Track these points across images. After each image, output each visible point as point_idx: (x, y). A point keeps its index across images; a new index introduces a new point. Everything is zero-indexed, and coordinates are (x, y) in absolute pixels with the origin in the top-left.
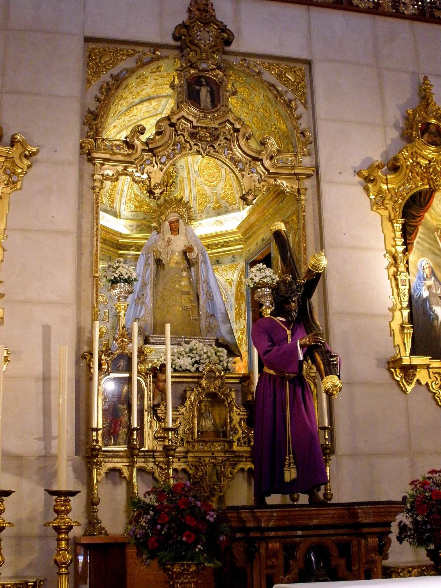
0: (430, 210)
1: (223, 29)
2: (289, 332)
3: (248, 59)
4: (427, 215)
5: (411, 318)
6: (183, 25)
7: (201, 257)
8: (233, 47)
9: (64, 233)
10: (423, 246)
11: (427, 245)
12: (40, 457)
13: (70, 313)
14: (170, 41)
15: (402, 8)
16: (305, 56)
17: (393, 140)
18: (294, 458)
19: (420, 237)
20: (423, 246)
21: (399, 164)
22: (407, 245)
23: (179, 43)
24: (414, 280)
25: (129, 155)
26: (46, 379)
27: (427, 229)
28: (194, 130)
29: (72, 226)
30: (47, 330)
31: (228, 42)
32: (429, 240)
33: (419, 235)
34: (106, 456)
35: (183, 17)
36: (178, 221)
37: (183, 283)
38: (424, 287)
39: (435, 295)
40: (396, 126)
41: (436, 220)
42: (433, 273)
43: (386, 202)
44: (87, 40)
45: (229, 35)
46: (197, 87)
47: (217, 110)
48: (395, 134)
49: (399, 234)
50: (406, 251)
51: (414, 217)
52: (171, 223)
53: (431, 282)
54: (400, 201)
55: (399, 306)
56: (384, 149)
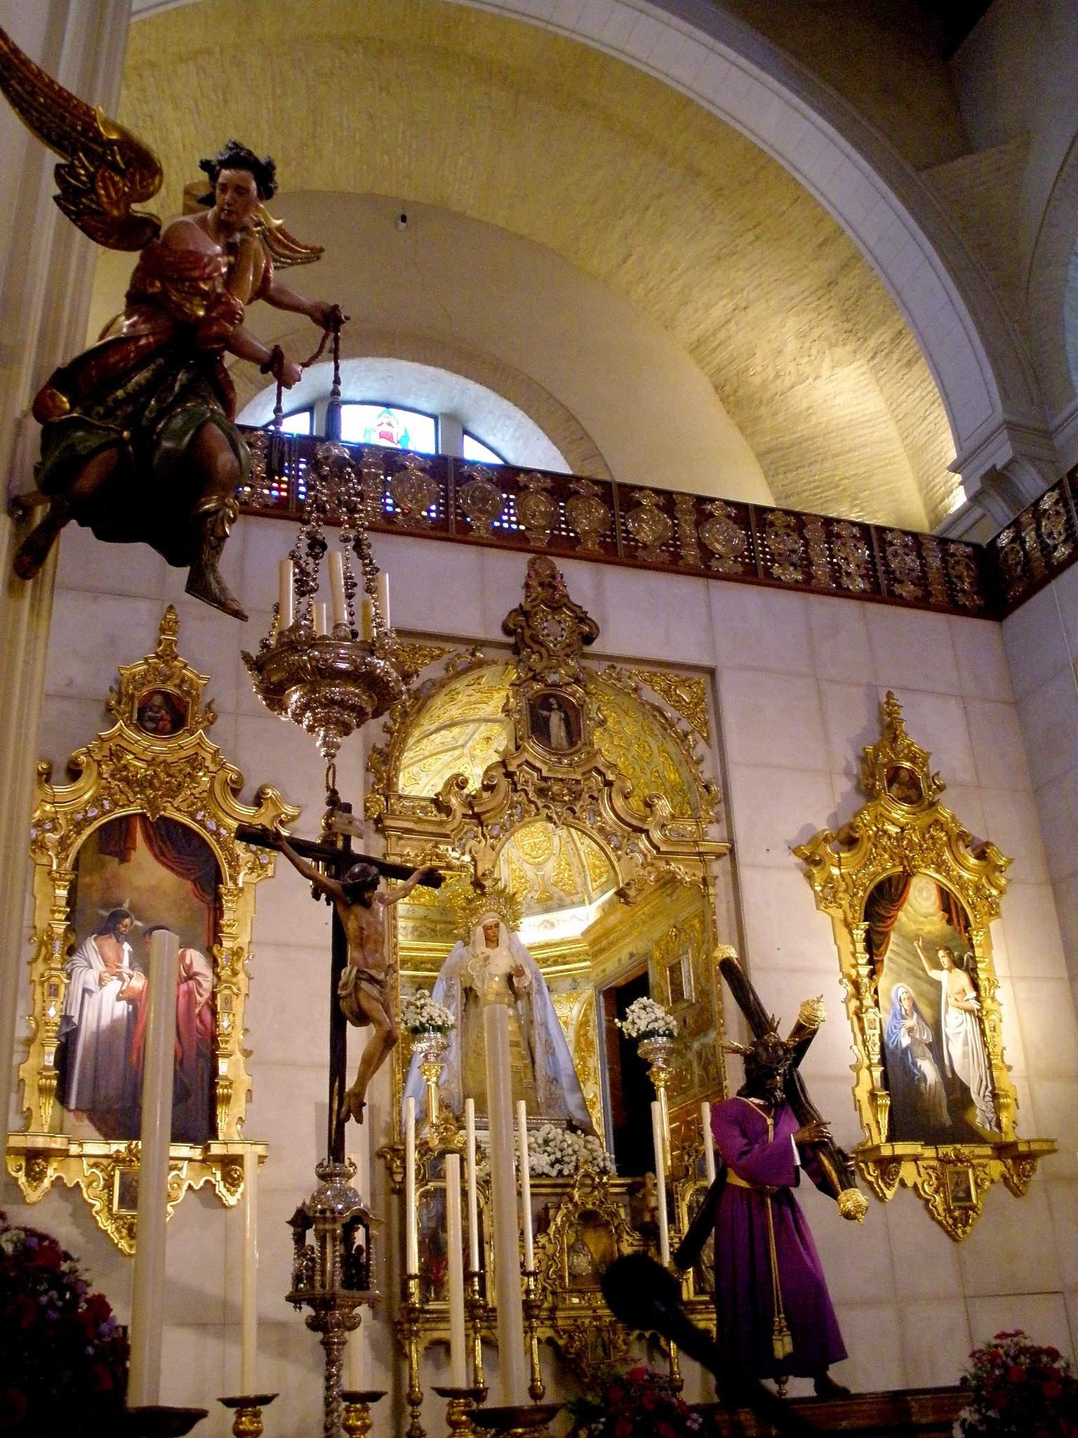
0: (906, 906)
1: (582, 618)
2: (770, 1121)
3: (619, 666)
4: (901, 914)
6: (520, 611)
7: (535, 985)
8: (595, 647)
10: (898, 965)
11: (904, 962)
14: (498, 635)
15: (845, 581)
16: (706, 662)
17: (845, 796)
18: (786, 1319)
19: (892, 950)
20: (898, 965)
21: (857, 835)
23: (512, 640)
25: (441, 823)
27: (903, 936)
28: (543, 784)
31: (588, 639)
32: (907, 955)
33: (890, 947)
34: (428, 1321)
35: (516, 598)
36: (497, 926)
38: (903, 1030)
39: (920, 1042)
40: (847, 773)
41: (915, 922)
42: (915, 1007)
43: (841, 895)
45: (591, 628)
46: (545, 713)
47: (576, 752)
48: (845, 785)
49: (861, 946)
50: (872, 974)
51: (883, 919)
52: (486, 928)
53: (912, 1021)
54: (861, 893)
55: (866, 1062)
56: (832, 810)
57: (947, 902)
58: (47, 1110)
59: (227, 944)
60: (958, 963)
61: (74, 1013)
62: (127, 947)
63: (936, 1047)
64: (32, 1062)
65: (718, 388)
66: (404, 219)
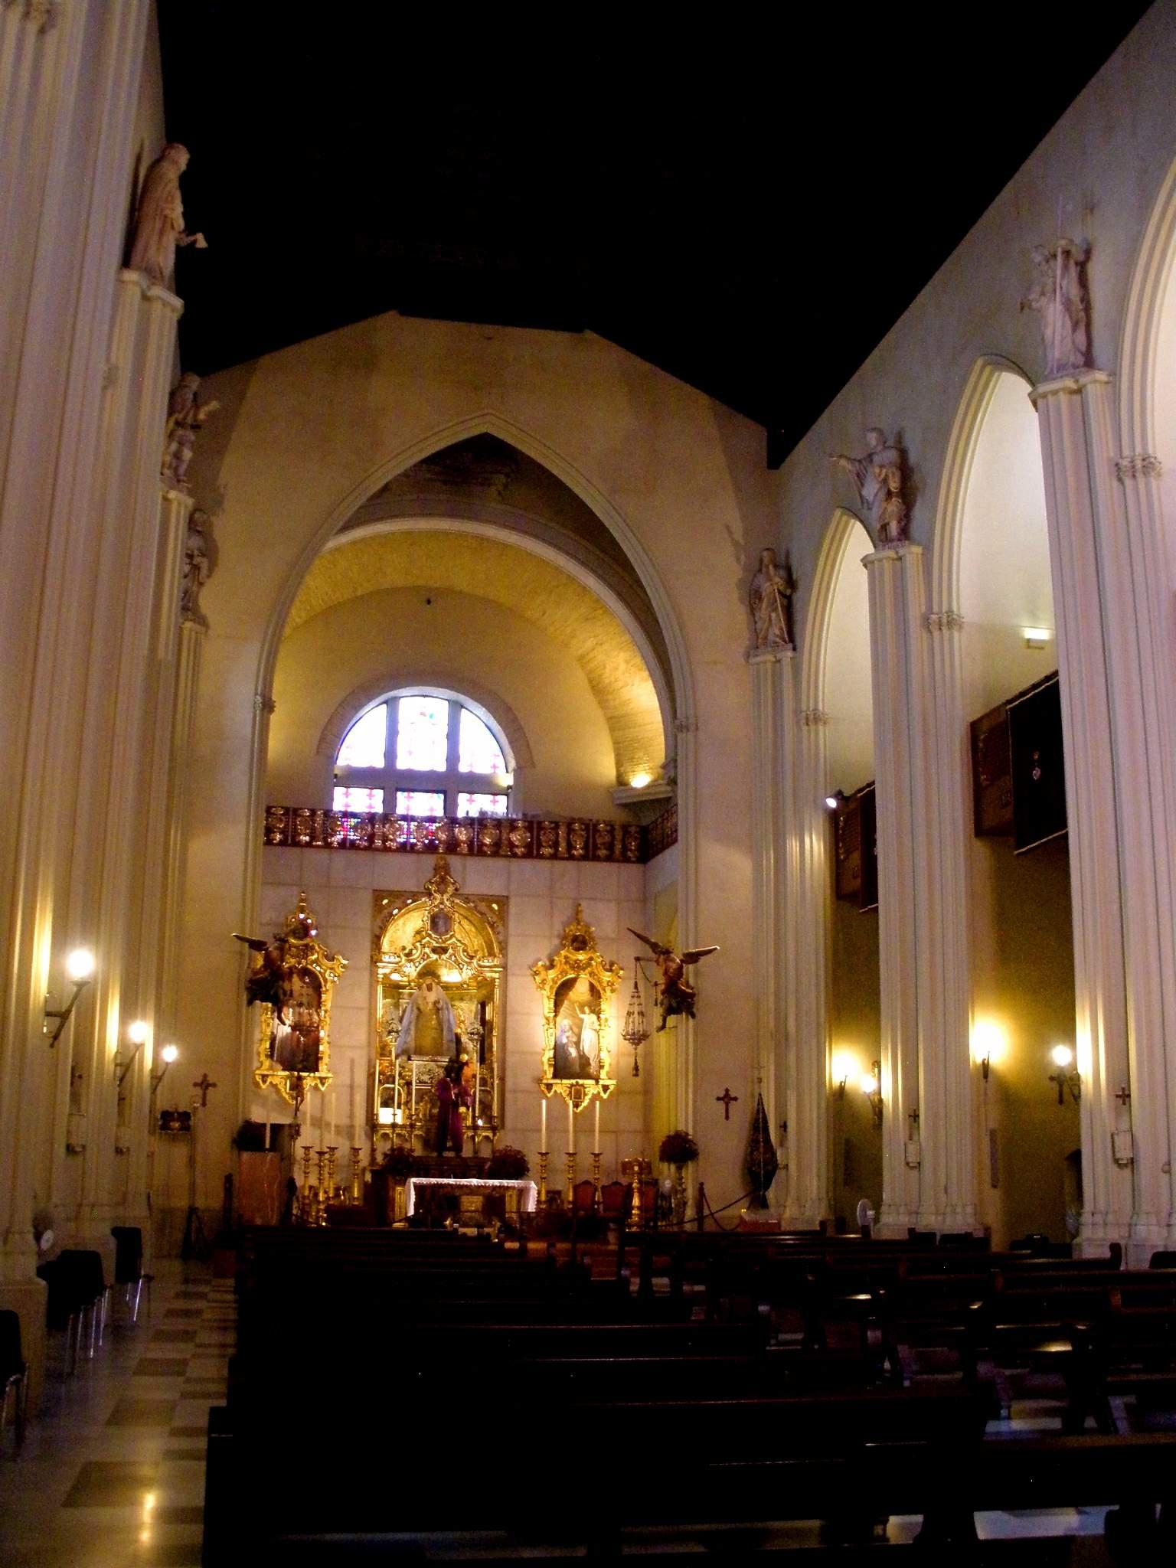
5: (555, 1057)
7: (445, 1006)
9: (362, 1009)
12: (347, 1127)
13: (364, 1052)
22: (556, 1012)
24: (559, 1033)
26: (352, 1087)
29: (365, 1005)
30: (352, 1061)
37: (433, 1022)
42: (571, 1029)
44: (375, 891)
48: (556, 942)
50: (556, 1016)
51: (563, 995)
52: (427, 985)
57: (592, 988)
58: (267, 1063)
59: (323, 1008)
60: (593, 1012)
61: (275, 1031)
62: (291, 1010)
63: (578, 1044)
64: (263, 1047)
65: (590, 681)
66: (429, 602)
